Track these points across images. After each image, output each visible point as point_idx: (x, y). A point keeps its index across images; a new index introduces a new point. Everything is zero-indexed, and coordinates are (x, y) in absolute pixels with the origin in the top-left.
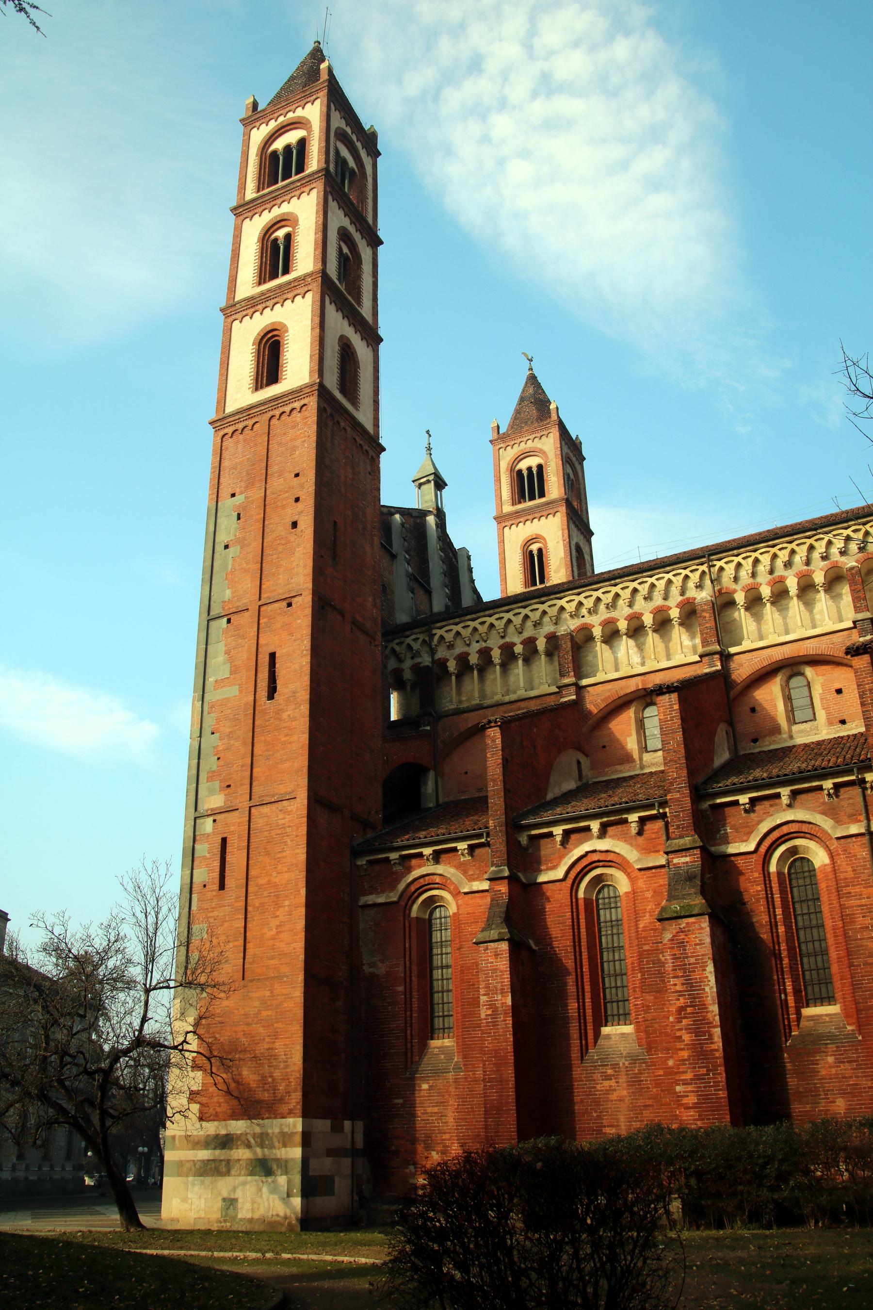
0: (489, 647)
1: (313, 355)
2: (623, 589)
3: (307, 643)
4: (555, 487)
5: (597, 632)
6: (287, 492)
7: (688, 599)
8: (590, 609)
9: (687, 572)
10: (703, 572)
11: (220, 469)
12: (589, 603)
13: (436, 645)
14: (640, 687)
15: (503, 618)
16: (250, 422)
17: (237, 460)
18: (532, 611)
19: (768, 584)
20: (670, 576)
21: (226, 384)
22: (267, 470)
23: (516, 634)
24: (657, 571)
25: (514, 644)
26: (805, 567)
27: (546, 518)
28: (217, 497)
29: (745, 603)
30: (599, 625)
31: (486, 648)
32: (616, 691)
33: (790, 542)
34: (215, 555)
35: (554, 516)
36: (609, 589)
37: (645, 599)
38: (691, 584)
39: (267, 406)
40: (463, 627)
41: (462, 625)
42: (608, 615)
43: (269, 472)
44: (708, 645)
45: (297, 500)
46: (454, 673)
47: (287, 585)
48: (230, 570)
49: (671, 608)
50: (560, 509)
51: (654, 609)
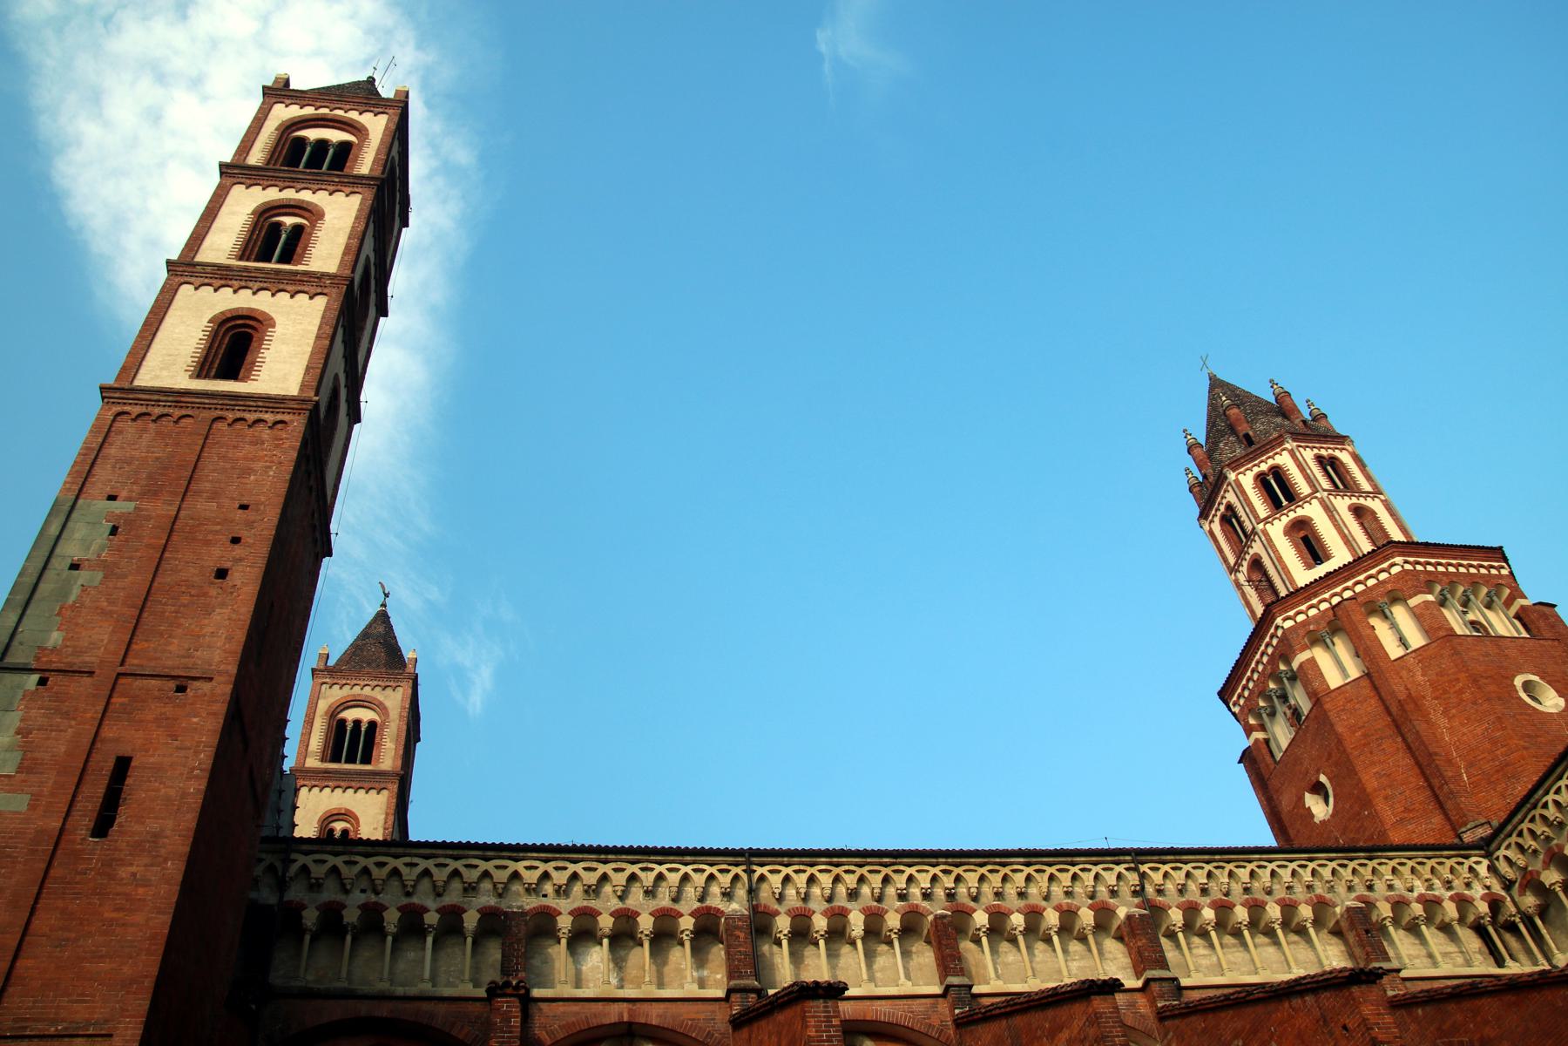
0: (381, 904)
1: (312, 368)
2: (616, 870)
3: (205, 758)
4: (387, 756)
5: (565, 923)
6: (218, 524)
7: (709, 908)
8: (560, 887)
9: (714, 870)
10: (736, 877)
11: (97, 455)
12: (561, 878)
13: (291, 878)
14: (625, 1019)
15: (416, 865)
16: (177, 413)
17: (136, 454)
18: (467, 866)
19: (824, 913)
20: (688, 869)
21: (147, 351)
22: (189, 483)
23: (432, 897)
24: (672, 858)
25: (426, 910)
26: (875, 904)
27: (367, 792)
28: (81, 490)
29: (789, 932)
30: (569, 913)
31: (376, 903)
32: (586, 1017)
33: (861, 866)
34: (47, 572)
35: (378, 793)
36: (594, 865)
37: (647, 893)
38: (715, 889)
39: (215, 401)
40: (346, 863)
41: (346, 858)
42: (585, 903)
43: (193, 487)
44: (740, 977)
45: (236, 540)
46: (311, 930)
47: (184, 657)
48: (70, 602)
49: (682, 915)
50: (389, 786)
51: (657, 910)
